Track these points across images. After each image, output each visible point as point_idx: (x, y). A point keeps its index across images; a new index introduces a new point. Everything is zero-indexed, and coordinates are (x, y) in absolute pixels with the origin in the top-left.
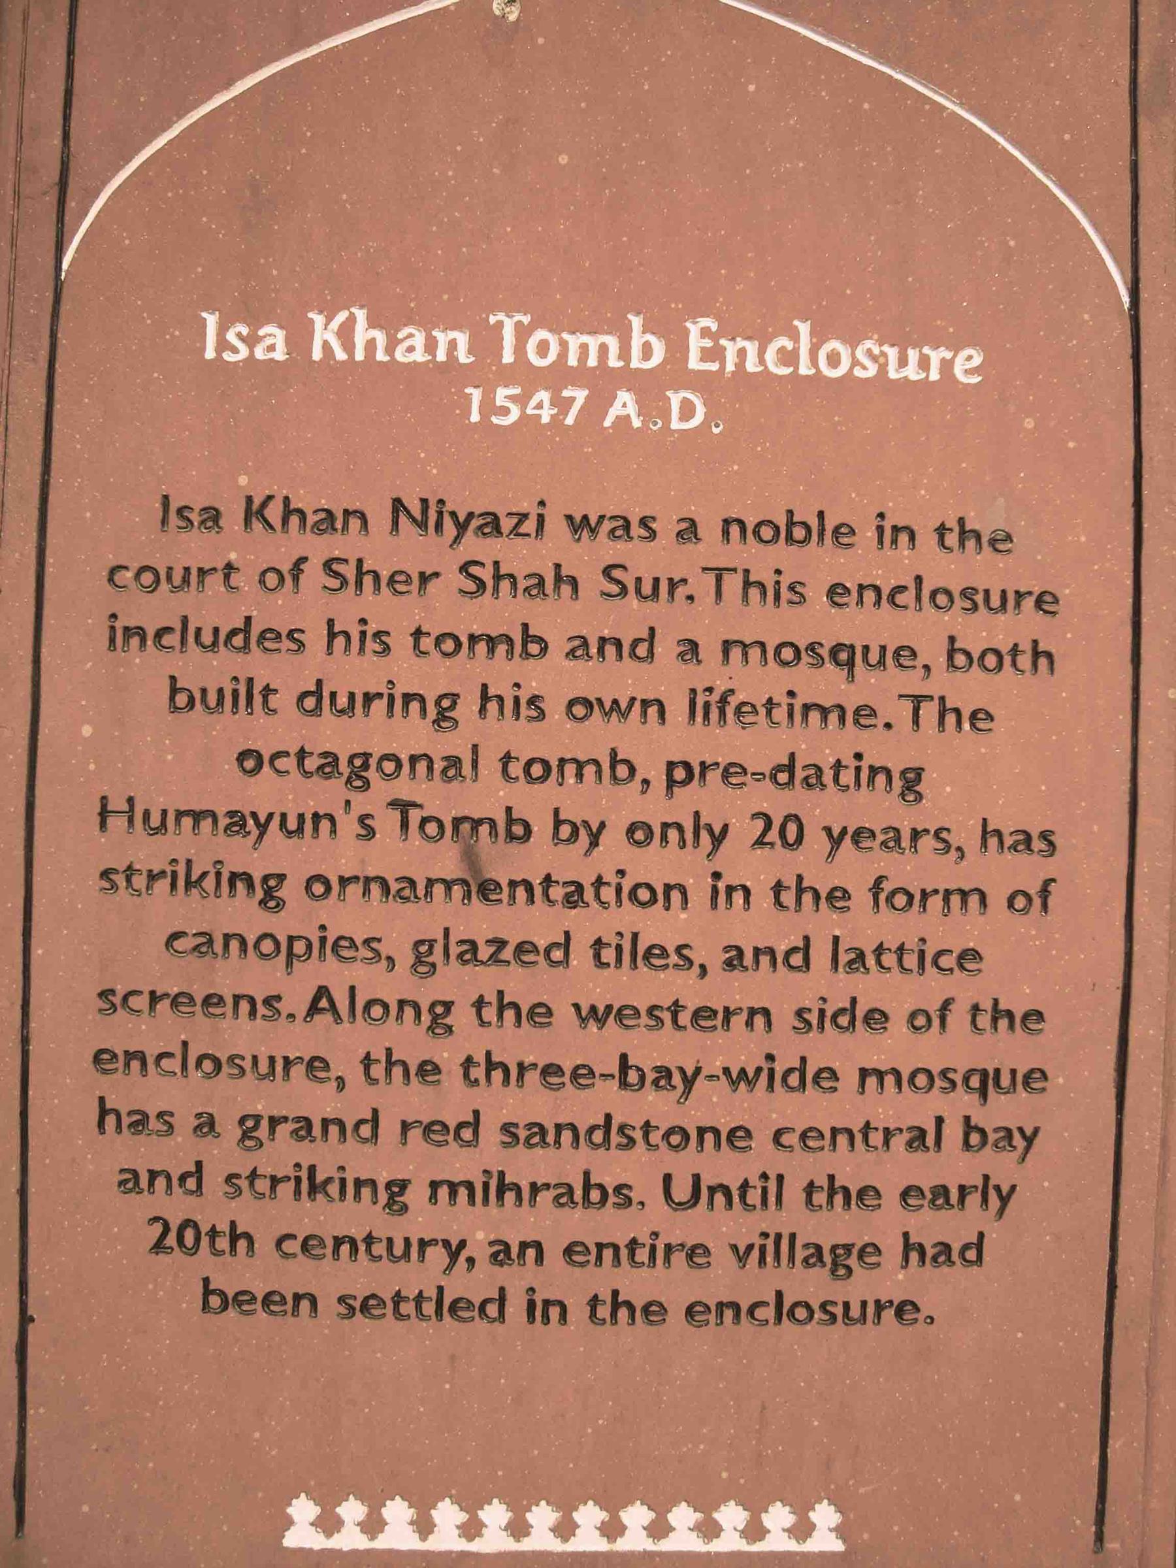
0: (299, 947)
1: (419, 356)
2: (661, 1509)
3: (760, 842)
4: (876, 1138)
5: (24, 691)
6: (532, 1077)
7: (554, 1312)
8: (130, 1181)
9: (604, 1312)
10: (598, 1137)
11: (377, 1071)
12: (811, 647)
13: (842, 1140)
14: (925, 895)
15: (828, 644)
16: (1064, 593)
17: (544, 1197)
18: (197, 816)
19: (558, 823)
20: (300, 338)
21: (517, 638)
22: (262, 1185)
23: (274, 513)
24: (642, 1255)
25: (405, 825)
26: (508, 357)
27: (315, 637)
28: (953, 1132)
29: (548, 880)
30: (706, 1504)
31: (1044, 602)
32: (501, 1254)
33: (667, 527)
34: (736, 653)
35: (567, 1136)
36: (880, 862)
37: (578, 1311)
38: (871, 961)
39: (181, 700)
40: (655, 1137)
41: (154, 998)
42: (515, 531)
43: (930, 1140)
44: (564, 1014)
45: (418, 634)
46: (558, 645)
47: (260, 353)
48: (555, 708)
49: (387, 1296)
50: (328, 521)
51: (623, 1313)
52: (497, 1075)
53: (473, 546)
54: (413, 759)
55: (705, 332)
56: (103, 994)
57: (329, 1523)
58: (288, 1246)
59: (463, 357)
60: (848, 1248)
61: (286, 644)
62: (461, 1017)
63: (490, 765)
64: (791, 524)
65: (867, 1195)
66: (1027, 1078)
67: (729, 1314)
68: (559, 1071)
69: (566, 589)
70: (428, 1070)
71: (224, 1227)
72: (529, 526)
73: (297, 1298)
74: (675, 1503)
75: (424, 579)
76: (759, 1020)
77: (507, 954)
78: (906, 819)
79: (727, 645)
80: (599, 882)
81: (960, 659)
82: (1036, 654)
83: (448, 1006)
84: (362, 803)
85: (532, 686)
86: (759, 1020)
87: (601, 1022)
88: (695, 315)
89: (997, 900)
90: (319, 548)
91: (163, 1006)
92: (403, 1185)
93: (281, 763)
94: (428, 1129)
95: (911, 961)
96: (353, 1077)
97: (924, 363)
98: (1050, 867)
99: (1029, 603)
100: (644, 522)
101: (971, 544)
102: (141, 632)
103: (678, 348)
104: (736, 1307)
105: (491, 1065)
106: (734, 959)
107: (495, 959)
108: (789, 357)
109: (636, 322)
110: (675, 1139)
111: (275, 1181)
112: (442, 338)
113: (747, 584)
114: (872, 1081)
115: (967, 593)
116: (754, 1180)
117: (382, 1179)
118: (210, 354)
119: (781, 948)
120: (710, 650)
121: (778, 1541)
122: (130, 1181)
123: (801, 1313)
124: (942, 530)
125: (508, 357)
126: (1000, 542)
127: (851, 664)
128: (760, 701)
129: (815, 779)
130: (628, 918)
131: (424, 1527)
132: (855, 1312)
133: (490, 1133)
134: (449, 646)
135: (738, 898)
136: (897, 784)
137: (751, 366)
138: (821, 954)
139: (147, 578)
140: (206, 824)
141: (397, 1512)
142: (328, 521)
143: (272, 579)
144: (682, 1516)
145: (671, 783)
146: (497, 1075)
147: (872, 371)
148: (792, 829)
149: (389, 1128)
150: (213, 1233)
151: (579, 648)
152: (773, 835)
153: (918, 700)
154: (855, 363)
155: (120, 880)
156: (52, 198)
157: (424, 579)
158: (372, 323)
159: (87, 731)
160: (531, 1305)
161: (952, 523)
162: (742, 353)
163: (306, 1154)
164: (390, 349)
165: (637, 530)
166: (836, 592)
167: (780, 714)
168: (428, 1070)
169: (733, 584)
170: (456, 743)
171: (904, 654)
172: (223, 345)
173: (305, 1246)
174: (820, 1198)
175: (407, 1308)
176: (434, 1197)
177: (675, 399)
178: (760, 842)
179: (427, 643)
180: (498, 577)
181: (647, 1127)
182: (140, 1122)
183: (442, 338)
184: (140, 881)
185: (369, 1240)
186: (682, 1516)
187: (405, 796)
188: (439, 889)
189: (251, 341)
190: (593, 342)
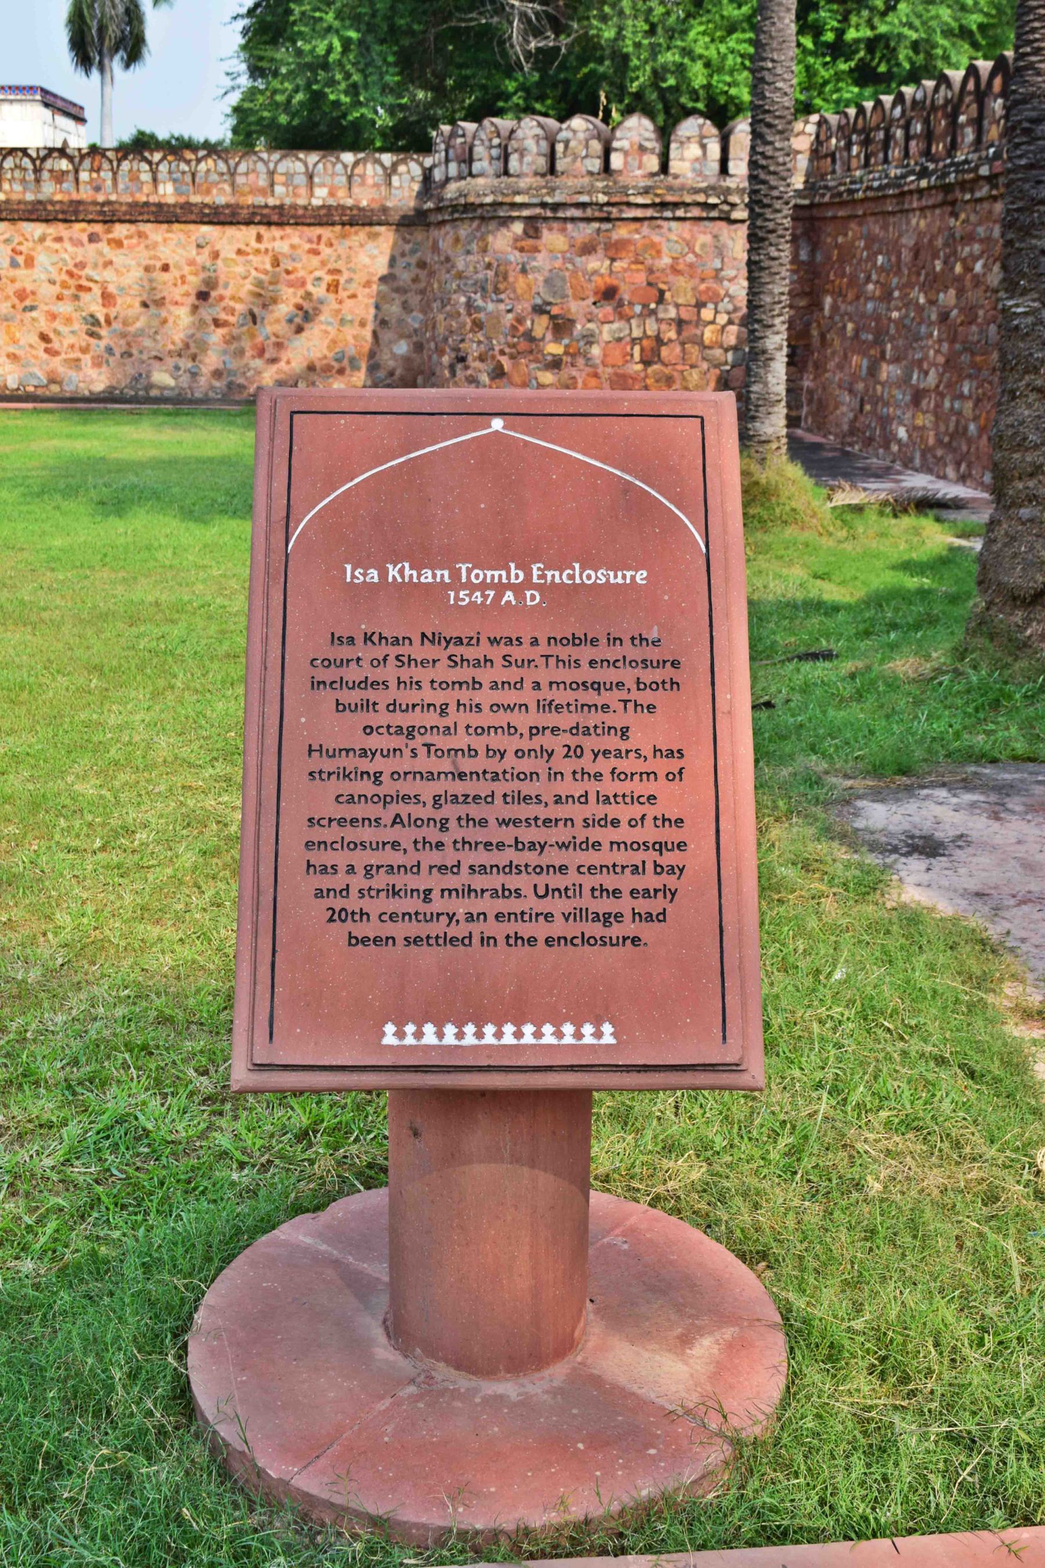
0: (388, 799)
1: (430, 580)
2: (539, 1026)
3: (566, 756)
4: (618, 869)
5: (278, 707)
6: (481, 847)
7: (492, 941)
8: (319, 894)
9: (512, 941)
10: (507, 870)
11: (420, 846)
12: (583, 684)
13: (605, 870)
14: (632, 774)
15: (590, 682)
16: (683, 660)
17: (487, 894)
18: (348, 751)
19: (488, 750)
20: (383, 573)
21: (470, 682)
22: (373, 893)
23: (375, 638)
24: (526, 917)
25: (429, 751)
26: (464, 580)
27: (393, 684)
28: (650, 867)
29: (485, 772)
30: (557, 1025)
31: (675, 664)
32: (470, 917)
33: (526, 640)
34: (554, 686)
35: (495, 869)
36: (613, 762)
37: (501, 941)
38: (612, 800)
39: (341, 708)
40: (530, 869)
41: (330, 820)
42: (468, 644)
43: (640, 870)
44: (492, 822)
45: (432, 682)
46: (486, 685)
47: (368, 580)
48: (486, 708)
49: (424, 937)
50: (396, 641)
51: (519, 942)
52: (467, 846)
53: (452, 649)
54: (432, 728)
55: (539, 569)
56: (310, 820)
57: (400, 1034)
58: (384, 918)
59: (447, 580)
60: (610, 914)
61: (381, 686)
62: (452, 824)
63: (461, 730)
64: (574, 638)
65: (616, 893)
66: (679, 846)
67: (562, 941)
68: (491, 844)
69: (489, 664)
70: (440, 845)
71: (357, 910)
72: (474, 641)
73: (387, 938)
74: (544, 1023)
75: (434, 661)
76: (569, 823)
77: (470, 800)
78: (623, 746)
79: (551, 683)
80: (505, 772)
81: (642, 686)
82: (672, 683)
83: (447, 820)
84: (412, 744)
85: (477, 700)
86: (569, 823)
87: (507, 825)
88: (535, 563)
89: (661, 775)
90: (393, 651)
91: (334, 823)
92: (430, 891)
93: (381, 730)
94: (440, 868)
95: (628, 800)
96: (410, 847)
97: (624, 577)
98: (682, 763)
99: (668, 664)
100: (517, 639)
101: (644, 643)
102: (324, 683)
103: (529, 575)
104: (565, 939)
105: (464, 843)
106: (558, 800)
107: (465, 802)
108: (571, 577)
109: (512, 565)
110: (538, 870)
111: (378, 891)
112: (439, 573)
113: (558, 661)
114: (615, 846)
115: (644, 661)
116: (570, 887)
117: (422, 889)
118: (348, 580)
119: (577, 795)
120: (545, 685)
121: (588, 1040)
122: (319, 894)
123: (592, 941)
124: (633, 639)
125: (464, 580)
126: (656, 643)
127: (599, 689)
128: (564, 704)
129: (587, 731)
130: (515, 785)
131: (440, 1035)
132: (614, 941)
133: (465, 869)
134: (444, 686)
135: (559, 777)
136: (619, 733)
137: (557, 580)
138: (592, 798)
139: (326, 663)
140: (351, 754)
141: (429, 1029)
142: (396, 641)
143: (375, 663)
144: (548, 1029)
145: (531, 734)
146: (467, 846)
147: (604, 580)
148: (579, 750)
149: (424, 867)
150: (353, 913)
151: (494, 686)
152: (571, 753)
153: (625, 702)
154: (597, 578)
155: (317, 776)
156: (283, 523)
157: (434, 661)
158: (411, 568)
159: (303, 720)
160: (482, 938)
161: (637, 636)
162: (553, 576)
163: (391, 879)
164: (419, 577)
165: (515, 642)
166: (592, 663)
167: (572, 708)
168: (440, 845)
169: (552, 661)
170: (448, 721)
171: (620, 685)
172: (353, 576)
173: (391, 918)
174: (597, 893)
175: (432, 941)
176: (442, 896)
177: (528, 594)
178: (566, 756)
179: (436, 685)
180: (462, 660)
181: (526, 866)
182: (324, 870)
183: (439, 573)
184: (325, 776)
185: (417, 914)
186: (548, 1029)
187: (429, 741)
188: (442, 776)
189: (365, 575)
190: (496, 573)
